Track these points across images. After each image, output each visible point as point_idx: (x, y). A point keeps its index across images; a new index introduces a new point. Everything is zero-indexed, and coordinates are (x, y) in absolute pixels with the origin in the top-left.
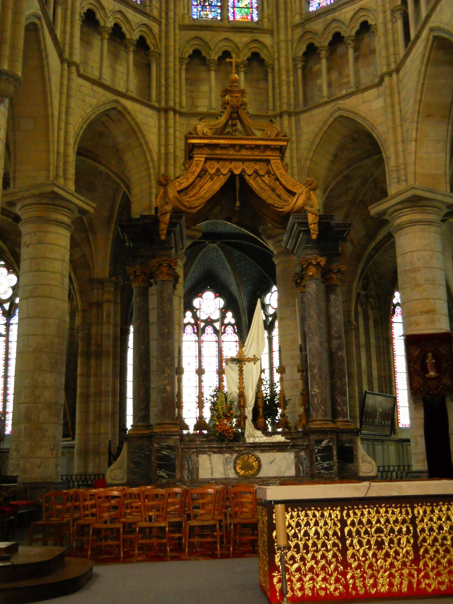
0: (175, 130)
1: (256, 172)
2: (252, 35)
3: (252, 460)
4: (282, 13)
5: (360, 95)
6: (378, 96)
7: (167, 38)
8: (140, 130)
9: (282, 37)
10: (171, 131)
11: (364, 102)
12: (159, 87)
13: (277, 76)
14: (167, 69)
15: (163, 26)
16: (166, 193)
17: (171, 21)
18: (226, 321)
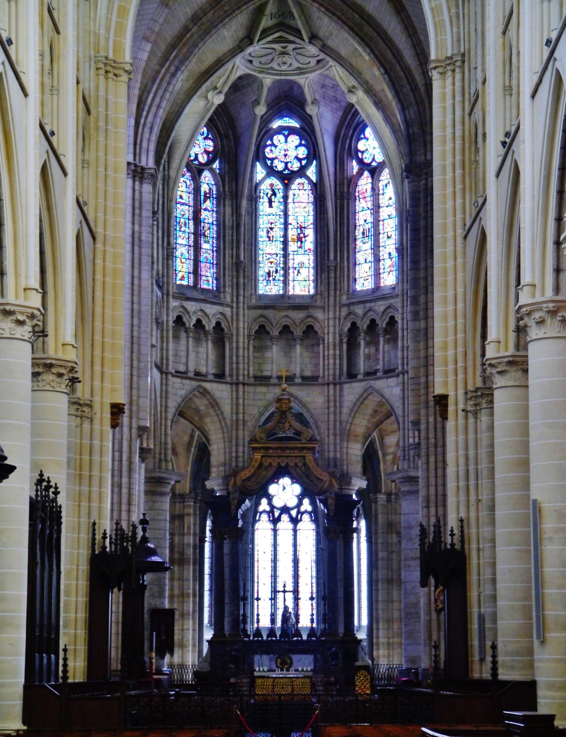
0: (244, 399)
1: (296, 464)
2: (307, 311)
3: (287, 658)
4: (332, 293)
5: (385, 380)
6: (397, 385)
7: (238, 320)
8: (217, 404)
9: (331, 315)
10: (241, 401)
11: (388, 387)
12: (231, 363)
13: (326, 349)
14: (237, 348)
15: (235, 309)
16: (235, 481)
17: (241, 305)
18: (303, 509)
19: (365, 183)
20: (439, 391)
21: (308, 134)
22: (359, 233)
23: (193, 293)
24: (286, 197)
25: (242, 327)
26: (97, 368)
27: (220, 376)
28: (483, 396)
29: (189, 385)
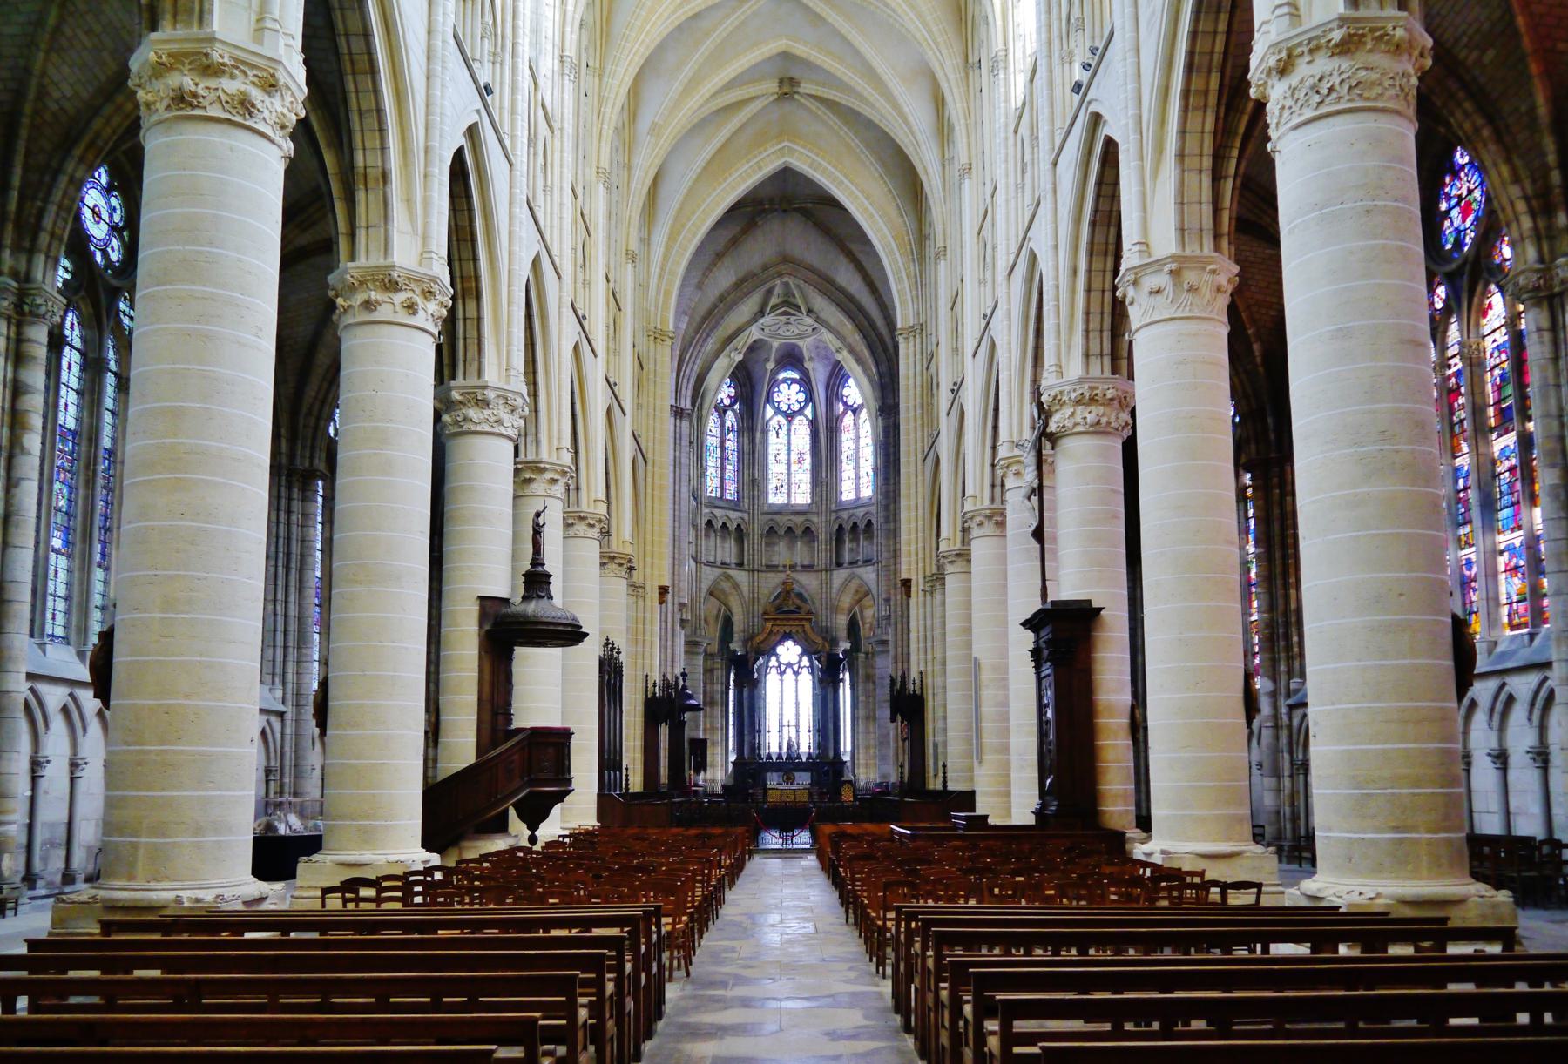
19: (848, 419)
20: (904, 576)
21: (806, 383)
22: (844, 457)
23: (720, 502)
24: (789, 430)
25: (757, 529)
26: (648, 559)
27: (740, 565)
28: (937, 579)
29: (718, 571)
